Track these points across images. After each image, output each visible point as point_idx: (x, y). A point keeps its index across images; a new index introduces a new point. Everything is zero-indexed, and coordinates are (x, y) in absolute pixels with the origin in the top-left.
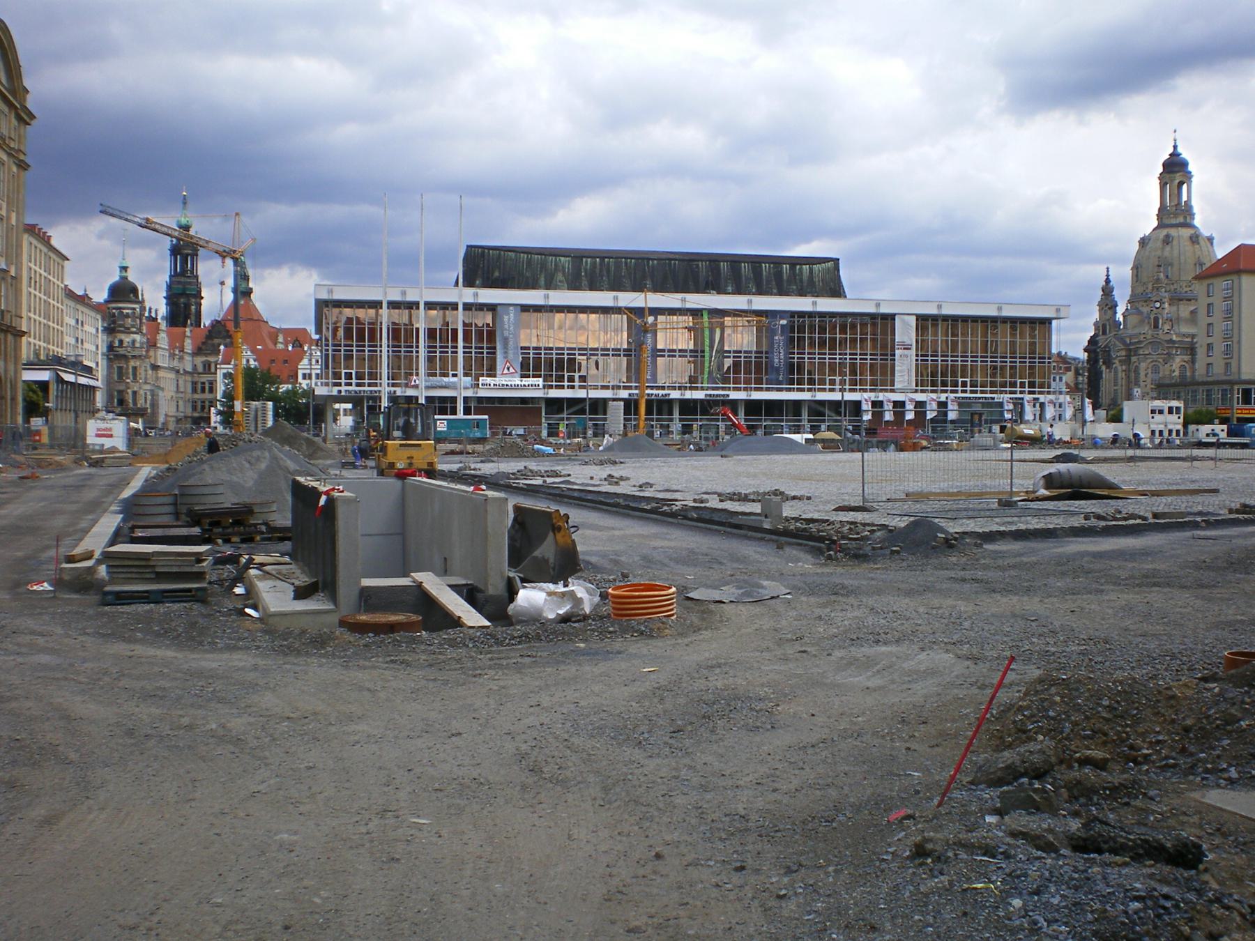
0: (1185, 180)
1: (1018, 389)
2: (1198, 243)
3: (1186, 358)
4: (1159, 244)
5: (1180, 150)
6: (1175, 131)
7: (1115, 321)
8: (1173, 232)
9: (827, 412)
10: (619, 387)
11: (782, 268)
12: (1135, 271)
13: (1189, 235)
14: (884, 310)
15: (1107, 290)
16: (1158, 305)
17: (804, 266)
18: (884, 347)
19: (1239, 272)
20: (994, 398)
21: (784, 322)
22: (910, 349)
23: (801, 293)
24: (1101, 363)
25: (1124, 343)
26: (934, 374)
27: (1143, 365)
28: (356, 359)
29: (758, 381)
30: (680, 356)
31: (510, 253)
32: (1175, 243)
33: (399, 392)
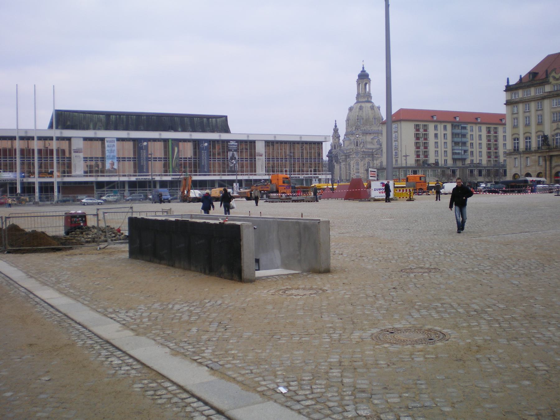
1: (309, 173)
2: (374, 110)
3: (370, 159)
4: (358, 110)
5: (365, 69)
7: (339, 143)
8: (363, 105)
9: (227, 185)
10: (131, 176)
11: (203, 120)
12: (347, 122)
13: (370, 106)
14: (251, 138)
15: (336, 130)
16: (357, 136)
17: (213, 119)
18: (251, 155)
19: (400, 121)
20: (299, 177)
21: (206, 144)
22: (262, 156)
23: (213, 131)
24: (334, 162)
25: (343, 152)
26: (273, 167)
27: (352, 162)
28: (3, 165)
29: (195, 171)
30: (159, 161)
31: (75, 113)
32: (364, 109)
33: (25, 180)
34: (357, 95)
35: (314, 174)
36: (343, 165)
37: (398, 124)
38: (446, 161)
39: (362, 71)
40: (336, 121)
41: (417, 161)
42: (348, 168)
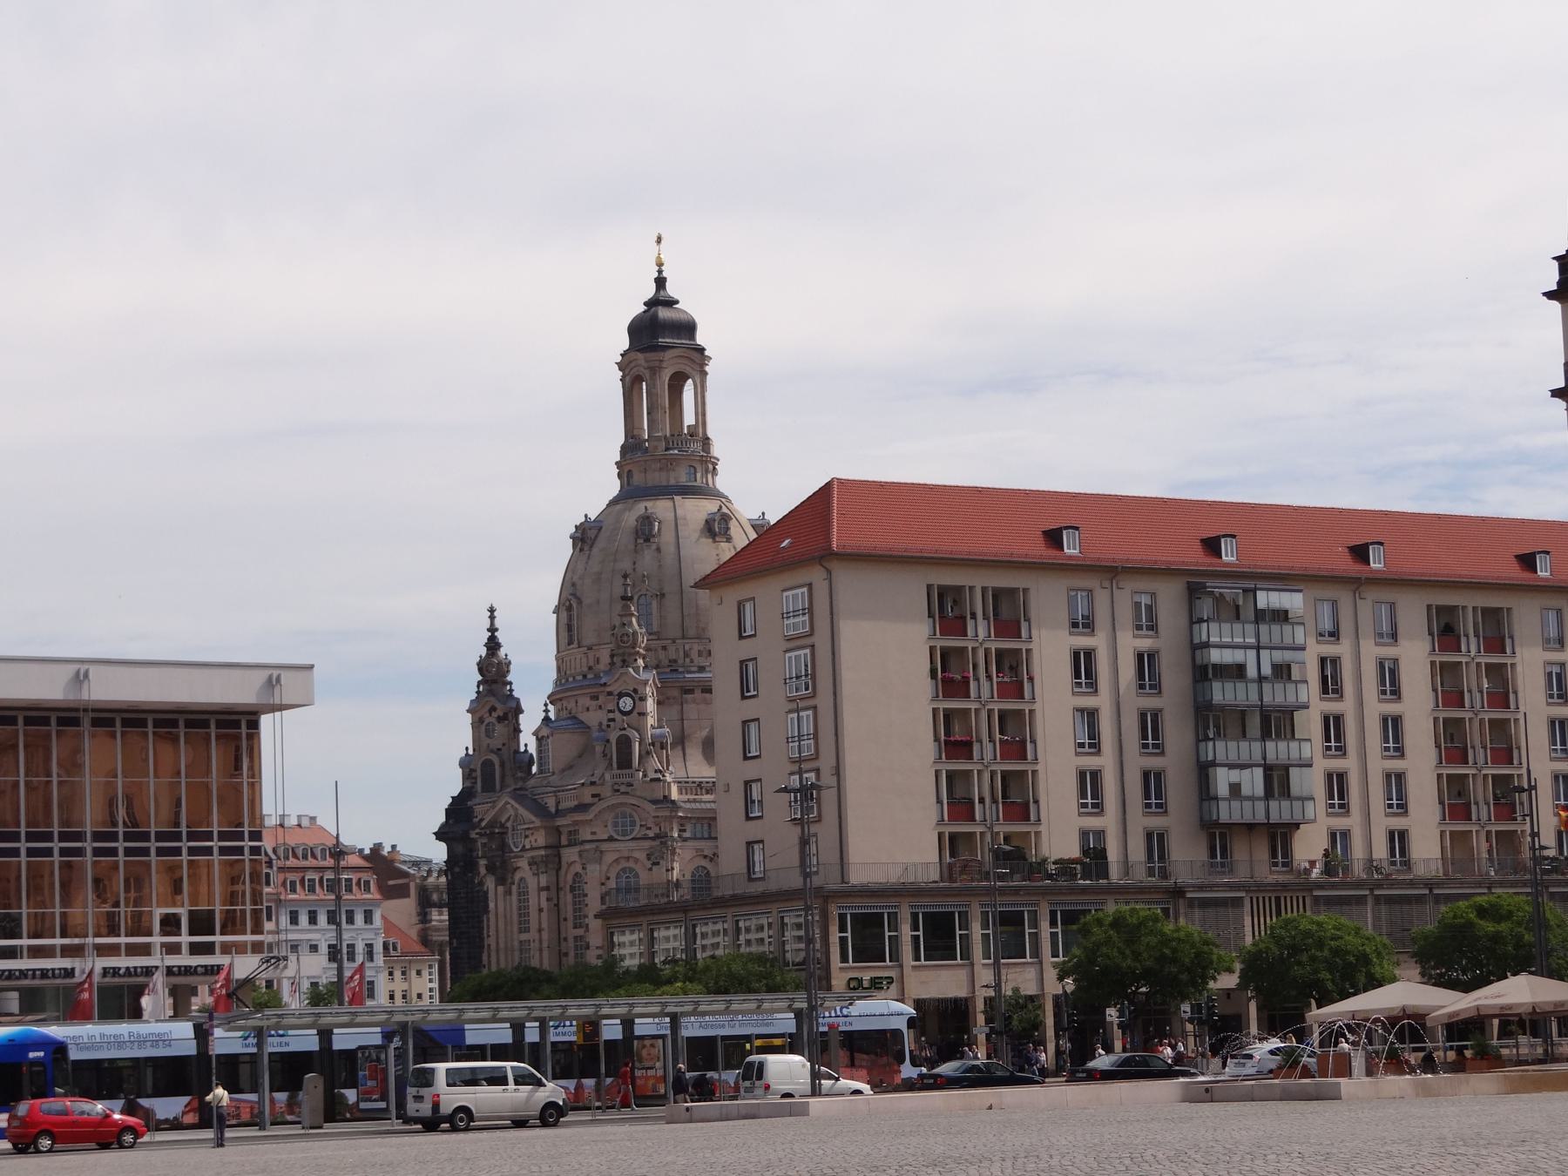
0: (688, 370)
1: (157, 939)
5: (672, 290)
6: (659, 240)
7: (517, 751)
12: (564, 615)
13: (703, 516)
15: (493, 671)
16: (627, 704)
19: (825, 556)
24: (483, 871)
27: (594, 872)
34: (624, 450)
35: (196, 949)
36: (541, 889)
37: (810, 586)
38: (1156, 843)
39: (651, 304)
40: (492, 610)
41: (953, 844)
42: (568, 911)
